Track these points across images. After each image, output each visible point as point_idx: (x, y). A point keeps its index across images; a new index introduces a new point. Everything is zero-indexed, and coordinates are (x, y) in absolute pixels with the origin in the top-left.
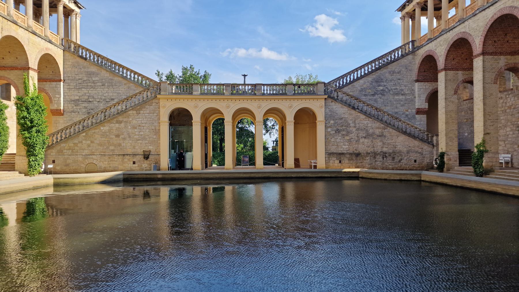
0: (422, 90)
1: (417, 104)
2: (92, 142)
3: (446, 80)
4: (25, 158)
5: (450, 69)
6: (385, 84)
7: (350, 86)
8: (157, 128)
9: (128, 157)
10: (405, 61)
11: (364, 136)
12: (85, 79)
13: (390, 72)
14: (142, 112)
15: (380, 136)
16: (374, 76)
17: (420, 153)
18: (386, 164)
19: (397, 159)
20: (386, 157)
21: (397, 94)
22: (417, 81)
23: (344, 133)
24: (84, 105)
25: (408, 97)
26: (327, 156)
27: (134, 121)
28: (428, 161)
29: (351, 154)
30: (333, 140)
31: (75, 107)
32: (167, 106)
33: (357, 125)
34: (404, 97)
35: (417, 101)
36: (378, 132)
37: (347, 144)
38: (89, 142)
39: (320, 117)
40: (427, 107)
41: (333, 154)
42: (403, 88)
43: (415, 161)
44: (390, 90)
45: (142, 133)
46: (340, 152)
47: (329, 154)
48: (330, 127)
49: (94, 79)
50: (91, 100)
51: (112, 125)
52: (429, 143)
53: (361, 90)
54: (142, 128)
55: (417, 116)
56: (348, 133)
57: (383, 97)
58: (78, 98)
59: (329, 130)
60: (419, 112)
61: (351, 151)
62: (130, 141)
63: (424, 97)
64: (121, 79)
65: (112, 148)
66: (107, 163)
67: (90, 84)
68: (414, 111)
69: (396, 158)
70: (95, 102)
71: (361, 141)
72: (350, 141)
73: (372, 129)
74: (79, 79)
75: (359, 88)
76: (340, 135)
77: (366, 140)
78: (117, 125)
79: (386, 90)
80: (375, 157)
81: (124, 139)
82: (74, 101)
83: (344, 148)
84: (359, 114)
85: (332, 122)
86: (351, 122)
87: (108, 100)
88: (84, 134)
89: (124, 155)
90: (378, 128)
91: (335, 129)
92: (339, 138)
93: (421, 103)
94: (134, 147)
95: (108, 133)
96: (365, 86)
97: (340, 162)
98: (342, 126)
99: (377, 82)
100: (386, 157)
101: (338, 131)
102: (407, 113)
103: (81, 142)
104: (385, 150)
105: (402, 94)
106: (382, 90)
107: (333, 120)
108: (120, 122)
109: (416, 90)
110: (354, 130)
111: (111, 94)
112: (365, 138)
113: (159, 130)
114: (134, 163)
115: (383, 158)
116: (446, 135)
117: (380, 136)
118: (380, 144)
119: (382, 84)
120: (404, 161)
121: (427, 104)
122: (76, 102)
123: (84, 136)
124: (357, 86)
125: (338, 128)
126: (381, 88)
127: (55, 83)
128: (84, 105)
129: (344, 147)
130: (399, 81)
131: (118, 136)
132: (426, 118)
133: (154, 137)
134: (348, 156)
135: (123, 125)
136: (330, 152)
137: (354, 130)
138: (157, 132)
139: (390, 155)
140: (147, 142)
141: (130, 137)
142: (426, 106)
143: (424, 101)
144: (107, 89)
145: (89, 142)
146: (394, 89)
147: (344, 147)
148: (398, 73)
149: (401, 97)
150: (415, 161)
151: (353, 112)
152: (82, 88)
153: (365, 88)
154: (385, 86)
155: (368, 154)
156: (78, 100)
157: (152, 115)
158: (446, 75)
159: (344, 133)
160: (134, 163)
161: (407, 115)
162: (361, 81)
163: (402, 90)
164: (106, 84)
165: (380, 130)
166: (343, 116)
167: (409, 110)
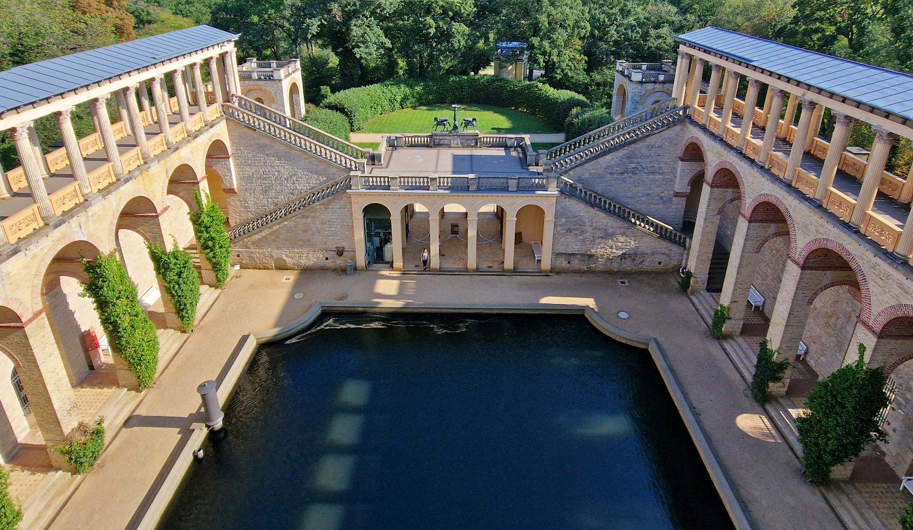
1: (676, 186)
22: (682, 160)
29: (583, 255)
39: (549, 217)
40: (688, 191)
47: (557, 255)
55: (674, 199)
56: (582, 232)
59: (559, 229)
60: (677, 195)
63: (687, 180)
71: (597, 241)
72: (583, 241)
78: (303, 220)
83: (575, 248)
85: (563, 220)
90: (620, 228)
91: (566, 227)
92: (570, 238)
93: (681, 185)
94: (325, 243)
101: (570, 230)
102: (663, 195)
108: (307, 217)
109: (679, 170)
110: (590, 229)
114: (327, 259)
131: (305, 231)
135: (309, 220)
137: (590, 229)
149: (657, 177)
151: (591, 209)
158: (711, 193)
160: (327, 259)
161: (661, 198)
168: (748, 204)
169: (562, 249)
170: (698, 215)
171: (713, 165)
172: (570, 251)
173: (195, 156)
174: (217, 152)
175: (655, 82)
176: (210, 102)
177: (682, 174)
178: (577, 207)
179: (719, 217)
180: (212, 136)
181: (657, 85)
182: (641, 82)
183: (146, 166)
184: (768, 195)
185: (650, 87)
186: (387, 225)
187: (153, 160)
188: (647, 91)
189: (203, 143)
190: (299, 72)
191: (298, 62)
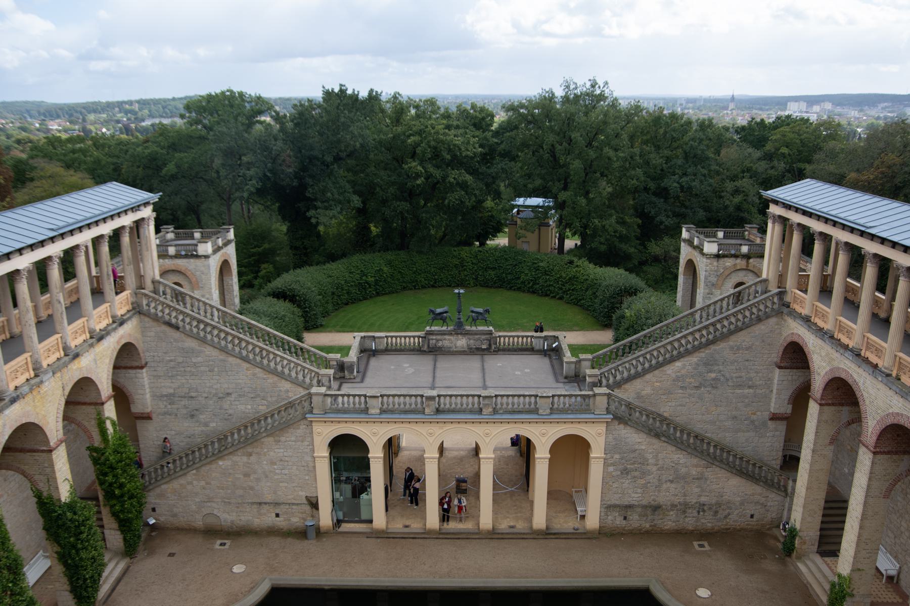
0: (785, 383)
1: (772, 405)
2: (207, 483)
3: (819, 422)
4: (119, 533)
5: (828, 405)
6: (721, 368)
7: (656, 372)
8: (311, 464)
9: (266, 507)
10: (763, 327)
11: (671, 478)
12: (180, 360)
13: (732, 348)
14: (283, 439)
15: (697, 479)
16: (703, 355)
17: (762, 504)
18: (703, 521)
19: (721, 515)
20: (704, 511)
21: (740, 386)
22: (780, 367)
23: (637, 474)
24: (183, 403)
25: (759, 391)
26: (603, 510)
27: (272, 453)
28: (774, 515)
29: (645, 507)
30: (615, 485)
31: (169, 406)
32: (324, 433)
33: (660, 462)
34: (751, 391)
35: (773, 400)
36: (694, 472)
37: (639, 491)
38: (203, 483)
39: (597, 452)
41: (615, 506)
42: (753, 375)
43: (752, 516)
44: (727, 380)
45: (286, 472)
46: (627, 503)
47: (608, 508)
48: (613, 464)
49: (194, 360)
50: (193, 394)
51: (235, 458)
52: (779, 489)
53: (677, 379)
54: (286, 463)
55: (770, 423)
56: (644, 474)
57: (714, 392)
58: (172, 391)
59: (611, 469)
60: (774, 418)
61: (645, 502)
62: (269, 484)
63: (787, 394)
64: (239, 361)
65: (240, 492)
66: (234, 514)
67: (189, 369)
68: (766, 415)
69: (720, 512)
70: (200, 398)
71: (665, 486)
72: (645, 487)
73: (686, 467)
74: (171, 361)
75: (674, 376)
76: (629, 477)
77: (673, 485)
78: (245, 459)
79: (722, 378)
80: (684, 512)
81: (258, 480)
82: (166, 396)
83: (634, 497)
84: (666, 444)
85: (617, 456)
86: (649, 456)
87: (221, 395)
88: (194, 471)
89: (260, 504)
90: (696, 466)
91: (622, 467)
92: (626, 483)
93: (778, 403)
94: (275, 493)
95: (231, 471)
96: (683, 372)
97: (625, 518)
98: (634, 464)
99: (706, 364)
100: (704, 511)
101: (625, 472)
102: (754, 417)
103: (191, 483)
104: (703, 499)
105: (750, 387)
106: (714, 379)
107: (620, 453)
108: (250, 455)
109: (776, 381)
110: (655, 468)
111: (226, 386)
112: (671, 482)
113: (314, 467)
114: (277, 515)
115: (699, 512)
116: (804, 507)
117: (697, 479)
118: (697, 490)
119: (716, 368)
120: (734, 517)
121: (790, 406)
122: (170, 398)
123: (194, 474)
124: (669, 372)
125: (625, 465)
126: (713, 375)
127: (134, 371)
128: (183, 403)
129: (633, 495)
130: (747, 363)
132: (785, 427)
133: (307, 478)
134: (639, 510)
135: (253, 459)
136: (609, 503)
137: (655, 468)
138: (312, 470)
139: (710, 508)
140: (294, 485)
141: (267, 477)
142: (788, 409)
143: (786, 401)
144: (218, 377)
145: (203, 483)
146: (737, 377)
147: (633, 495)
148: (747, 349)
149: (746, 391)
150: (752, 516)
152: (177, 375)
153: (682, 376)
154: (720, 371)
155: (673, 506)
156: (173, 395)
157: (299, 443)
158: (820, 413)
159: (637, 474)
160: (277, 515)
161: (753, 422)
162: (678, 364)
163: (750, 379)
164: (216, 369)
165: (699, 469)
166: (637, 447)
167: (759, 413)
168: (872, 426)
169: (615, 500)
170: (804, 445)
171: (822, 374)
172: (626, 501)
173: (98, 365)
174: (126, 358)
175: (735, 256)
176: (119, 289)
177: (778, 387)
178: (632, 437)
179: (832, 447)
180: (122, 337)
181: (739, 261)
182: (718, 256)
183: (37, 380)
184: (898, 414)
185: (729, 262)
186: (364, 464)
187: (46, 372)
188: (725, 268)
189: (110, 346)
190: (233, 245)
191: (232, 231)
